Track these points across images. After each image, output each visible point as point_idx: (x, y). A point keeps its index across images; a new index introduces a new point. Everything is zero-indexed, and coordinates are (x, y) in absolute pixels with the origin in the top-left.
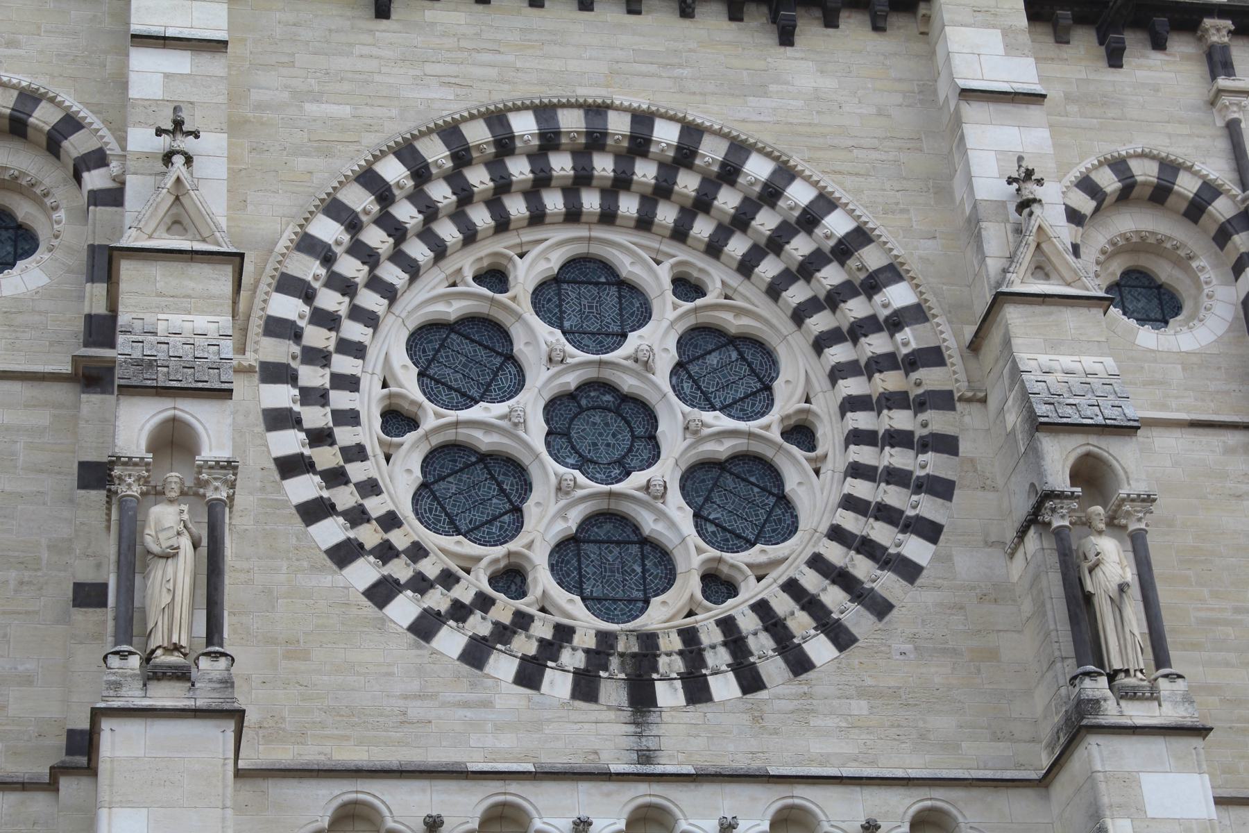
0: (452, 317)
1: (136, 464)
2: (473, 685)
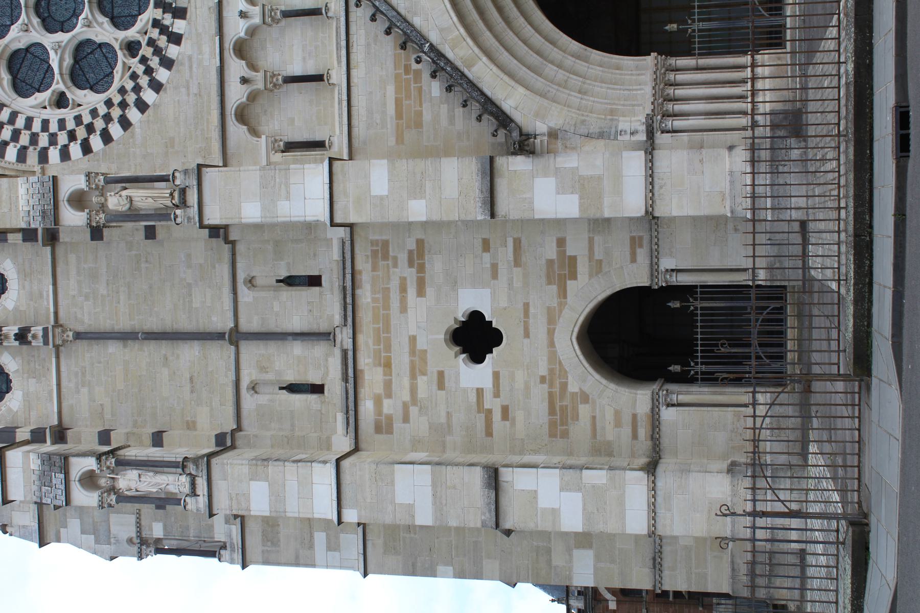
0: (10, 77)
1: (90, 216)
2: (182, 64)
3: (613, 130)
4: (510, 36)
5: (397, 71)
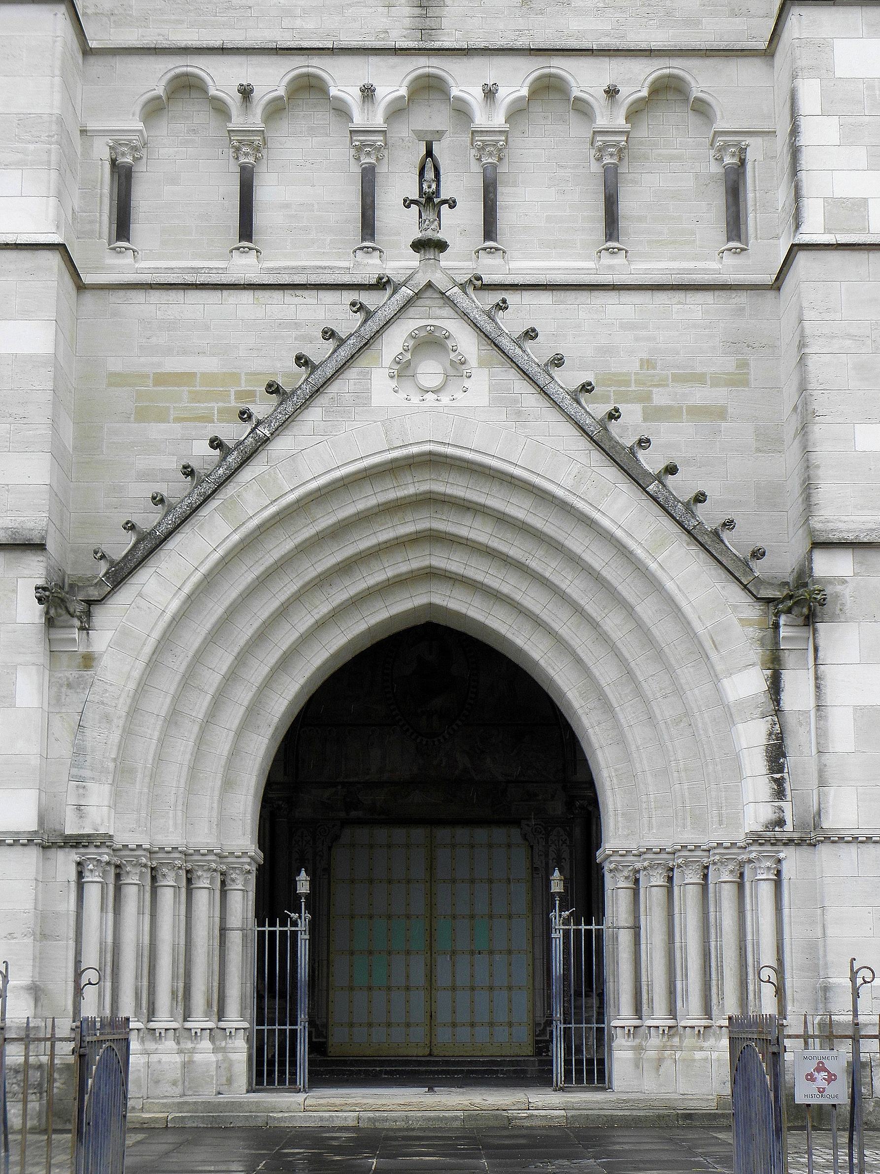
3: (87, 773)
4: (288, 587)
5: (243, 377)
